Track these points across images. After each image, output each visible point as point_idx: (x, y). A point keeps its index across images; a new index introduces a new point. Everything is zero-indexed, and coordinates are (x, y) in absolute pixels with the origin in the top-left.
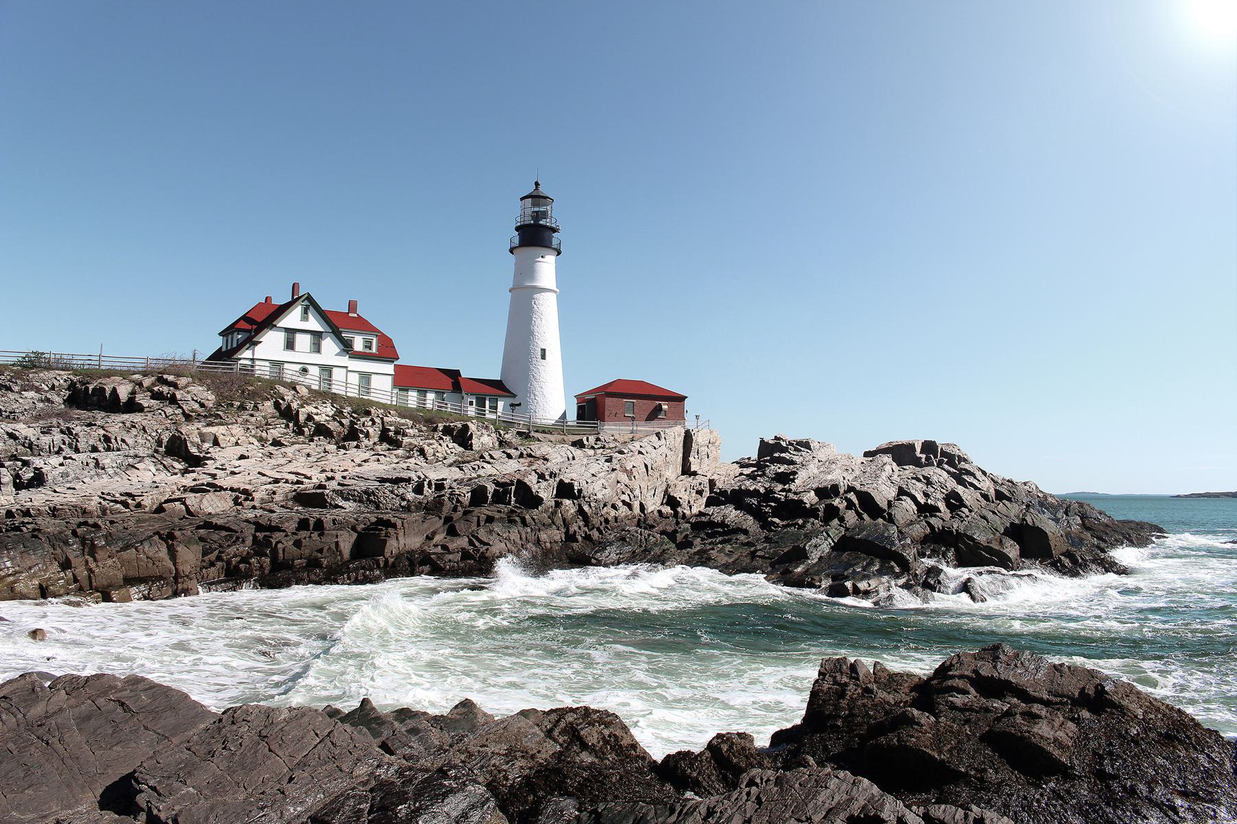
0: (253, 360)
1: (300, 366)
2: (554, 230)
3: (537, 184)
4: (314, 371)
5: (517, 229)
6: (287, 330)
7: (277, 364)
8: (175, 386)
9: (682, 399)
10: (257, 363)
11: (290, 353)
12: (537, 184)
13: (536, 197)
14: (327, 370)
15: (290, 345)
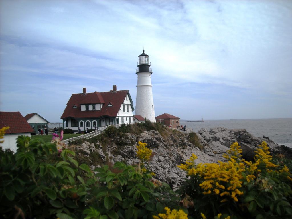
0: (119, 116)
1: (126, 117)
2: (150, 66)
3: (143, 51)
4: (128, 118)
5: (138, 66)
6: (123, 104)
7: (123, 117)
8: (157, 134)
9: (179, 119)
10: (120, 117)
11: (124, 113)
12: (143, 51)
13: (143, 54)
14: (130, 117)
15: (124, 111)
